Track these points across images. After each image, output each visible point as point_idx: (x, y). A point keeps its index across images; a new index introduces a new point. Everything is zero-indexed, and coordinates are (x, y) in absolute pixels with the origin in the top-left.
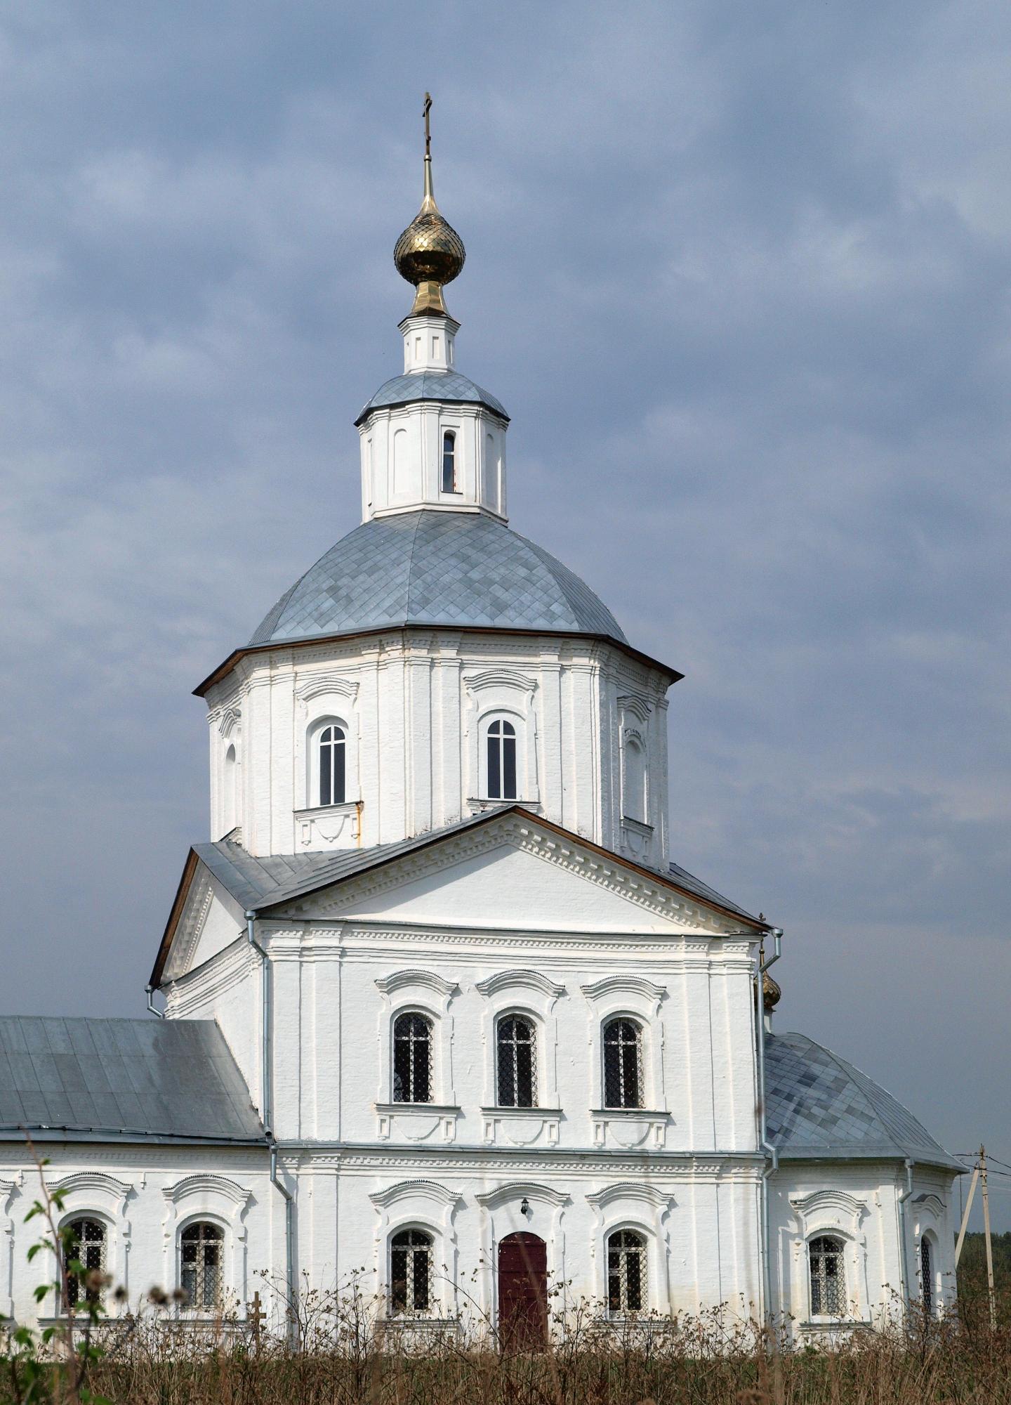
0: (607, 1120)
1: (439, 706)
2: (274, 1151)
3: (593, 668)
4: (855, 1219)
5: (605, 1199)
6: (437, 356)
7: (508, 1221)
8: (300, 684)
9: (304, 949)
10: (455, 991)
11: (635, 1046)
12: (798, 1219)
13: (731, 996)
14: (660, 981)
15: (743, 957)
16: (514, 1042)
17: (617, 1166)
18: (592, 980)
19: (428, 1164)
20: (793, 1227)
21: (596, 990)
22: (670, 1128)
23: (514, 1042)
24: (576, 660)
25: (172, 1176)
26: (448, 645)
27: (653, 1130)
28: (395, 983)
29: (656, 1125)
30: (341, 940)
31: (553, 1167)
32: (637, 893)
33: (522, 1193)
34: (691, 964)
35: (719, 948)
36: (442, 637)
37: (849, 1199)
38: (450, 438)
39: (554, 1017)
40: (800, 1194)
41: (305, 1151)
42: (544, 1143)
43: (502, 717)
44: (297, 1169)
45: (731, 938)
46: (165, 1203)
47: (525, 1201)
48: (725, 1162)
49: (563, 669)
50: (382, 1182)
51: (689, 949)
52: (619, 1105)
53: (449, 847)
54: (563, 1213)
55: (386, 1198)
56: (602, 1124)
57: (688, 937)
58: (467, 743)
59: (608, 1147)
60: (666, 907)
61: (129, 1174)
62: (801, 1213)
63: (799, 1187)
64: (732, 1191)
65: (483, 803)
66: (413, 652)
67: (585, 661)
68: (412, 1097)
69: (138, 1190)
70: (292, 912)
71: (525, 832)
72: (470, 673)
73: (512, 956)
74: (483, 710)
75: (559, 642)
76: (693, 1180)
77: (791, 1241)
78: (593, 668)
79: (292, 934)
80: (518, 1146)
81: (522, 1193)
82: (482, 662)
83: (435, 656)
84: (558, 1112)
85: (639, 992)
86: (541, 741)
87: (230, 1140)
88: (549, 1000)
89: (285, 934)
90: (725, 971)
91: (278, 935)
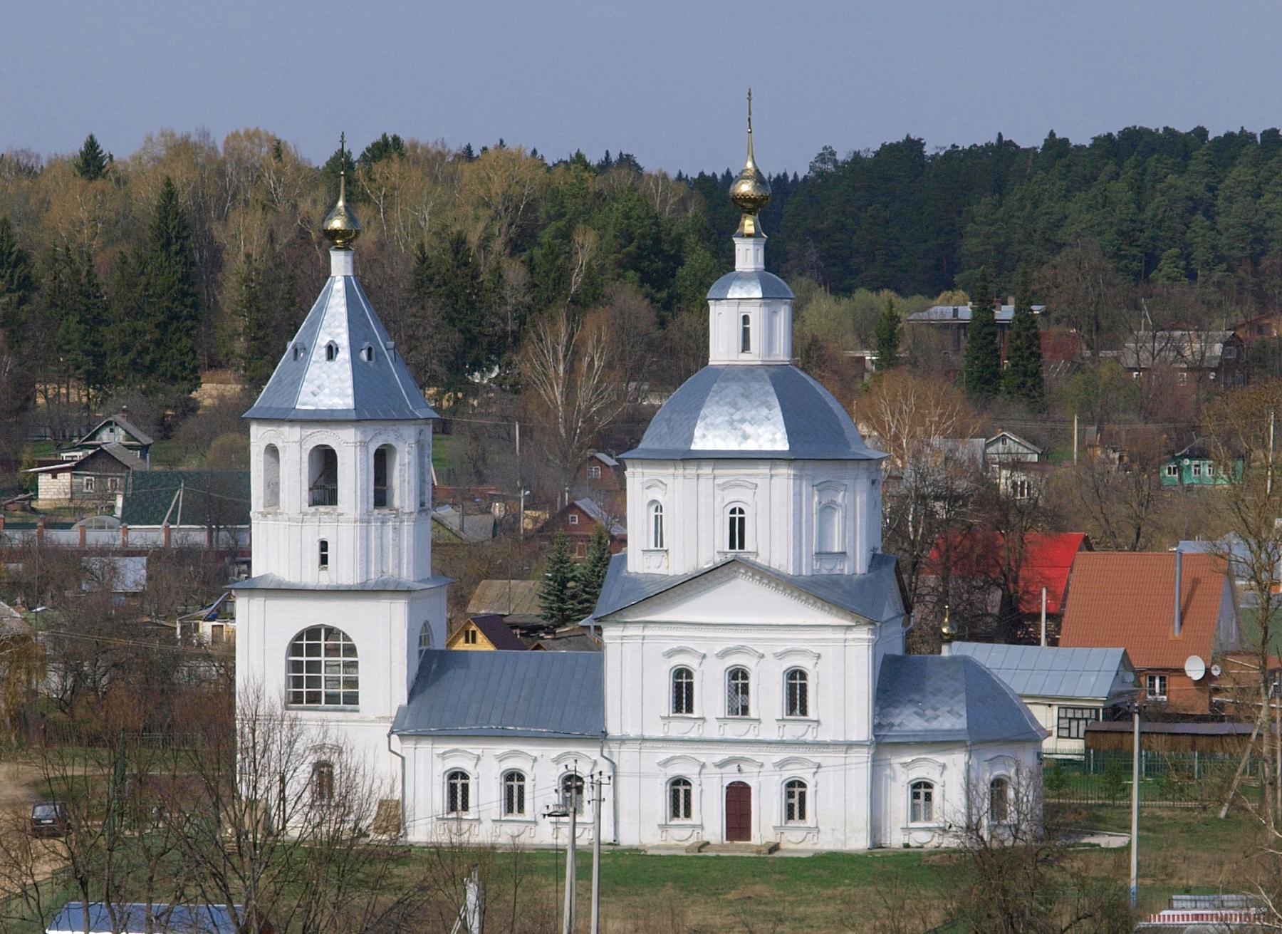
1: (702, 500)
3: (789, 475)
4: (938, 773)
5: (782, 765)
6: (749, 261)
7: (731, 776)
8: (645, 479)
10: (704, 656)
14: (817, 650)
16: (740, 681)
18: (779, 650)
23: (740, 681)
27: (810, 729)
28: (671, 654)
34: (835, 640)
36: (703, 463)
38: (746, 319)
41: (623, 740)
43: (737, 505)
45: (858, 624)
48: (850, 745)
49: (772, 476)
53: (709, 576)
58: (718, 520)
59: (784, 738)
65: (725, 553)
66: (688, 471)
69: (539, 759)
70: (617, 617)
72: (719, 481)
74: (726, 501)
78: (789, 475)
84: (758, 720)
86: (759, 518)
88: (755, 660)
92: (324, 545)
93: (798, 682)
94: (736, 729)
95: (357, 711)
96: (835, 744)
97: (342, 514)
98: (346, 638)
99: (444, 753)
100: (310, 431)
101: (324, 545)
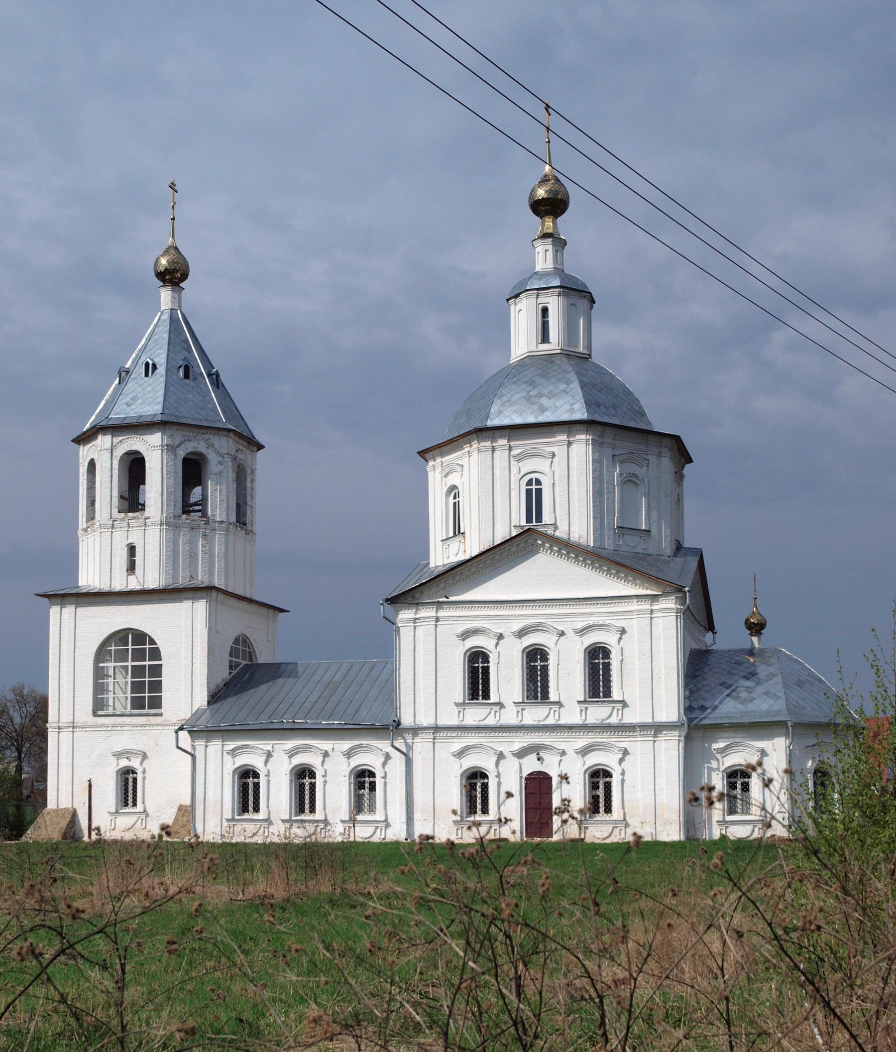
0: (586, 706)
1: (497, 473)
5: (585, 752)
7: (531, 765)
9: (416, 619)
10: (501, 637)
11: (609, 662)
12: (718, 760)
13: (664, 629)
14: (623, 624)
15: (673, 606)
17: (592, 732)
18: (580, 625)
19: (483, 735)
20: (714, 764)
21: (581, 631)
22: (626, 710)
23: (538, 663)
24: (578, 437)
25: (346, 745)
26: (502, 437)
30: (437, 613)
31: (554, 734)
32: (608, 572)
33: (535, 749)
35: (658, 601)
36: (497, 433)
37: (752, 747)
39: (558, 648)
40: (721, 745)
41: (416, 730)
42: (551, 721)
43: (534, 476)
44: (413, 739)
45: (665, 594)
46: (344, 759)
47: (538, 754)
48: (657, 728)
50: (457, 745)
51: (639, 603)
52: (600, 698)
54: (561, 760)
55: (460, 754)
56: (584, 708)
57: (637, 596)
58: (514, 494)
59: (586, 722)
60: (626, 580)
61: (325, 745)
62: (718, 756)
63: (720, 740)
64: (663, 745)
66: (483, 444)
67: (583, 437)
68: (481, 698)
69: (330, 752)
71: (539, 542)
73: (532, 615)
74: (522, 473)
75: (567, 427)
77: (713, 773)
78: (587, 440)
79: (410, 611)
80: (536, 723)
81: (535, 749)
82: (521, 446)
83: (494, 444)
85: (607, 631)
89: (406, 611)
90: (661, 615)
91: (403, 612)
92: (132, 549)
93: (601, 661)
94: (535, 714)
95: (161, 715)
96: (644, 727)
97: (149, 518)
98: (152, 642)
99: (234, 750)
100: (120, 438)
101: (132, 549)
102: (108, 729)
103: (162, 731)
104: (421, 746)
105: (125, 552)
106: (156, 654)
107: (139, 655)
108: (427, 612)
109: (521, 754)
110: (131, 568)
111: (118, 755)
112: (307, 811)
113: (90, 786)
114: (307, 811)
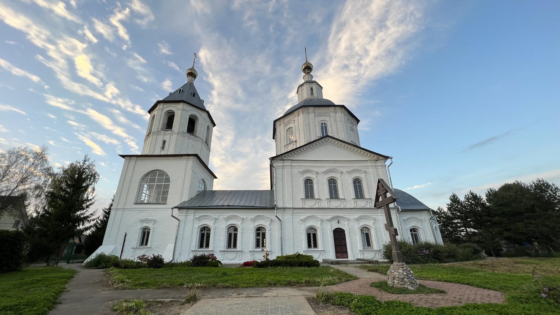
2: (276, 209)
5: (358, 219)
13: (382, 173)
29: (368, 202)
43: (324, 122)
54: (348, 223)
76: (380, 214)
87: (266, 207)
92: (164, 142)
101: (164, 142)
102: (140, 210)
103: (165, 211)
104: (287, 217)
105: (161, 143)
106: (168, 180)
107: (160, 181)
108: (287, 163)
109: (330, 220)
110: (163, 148)
111: (142, 221)
112: (232, 247)
113: (126, 235)
114: (232, 247)
